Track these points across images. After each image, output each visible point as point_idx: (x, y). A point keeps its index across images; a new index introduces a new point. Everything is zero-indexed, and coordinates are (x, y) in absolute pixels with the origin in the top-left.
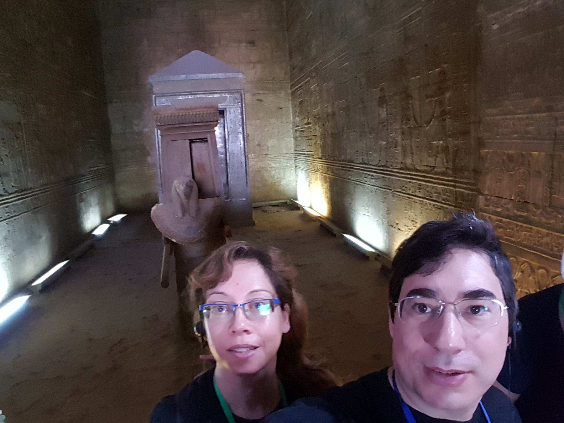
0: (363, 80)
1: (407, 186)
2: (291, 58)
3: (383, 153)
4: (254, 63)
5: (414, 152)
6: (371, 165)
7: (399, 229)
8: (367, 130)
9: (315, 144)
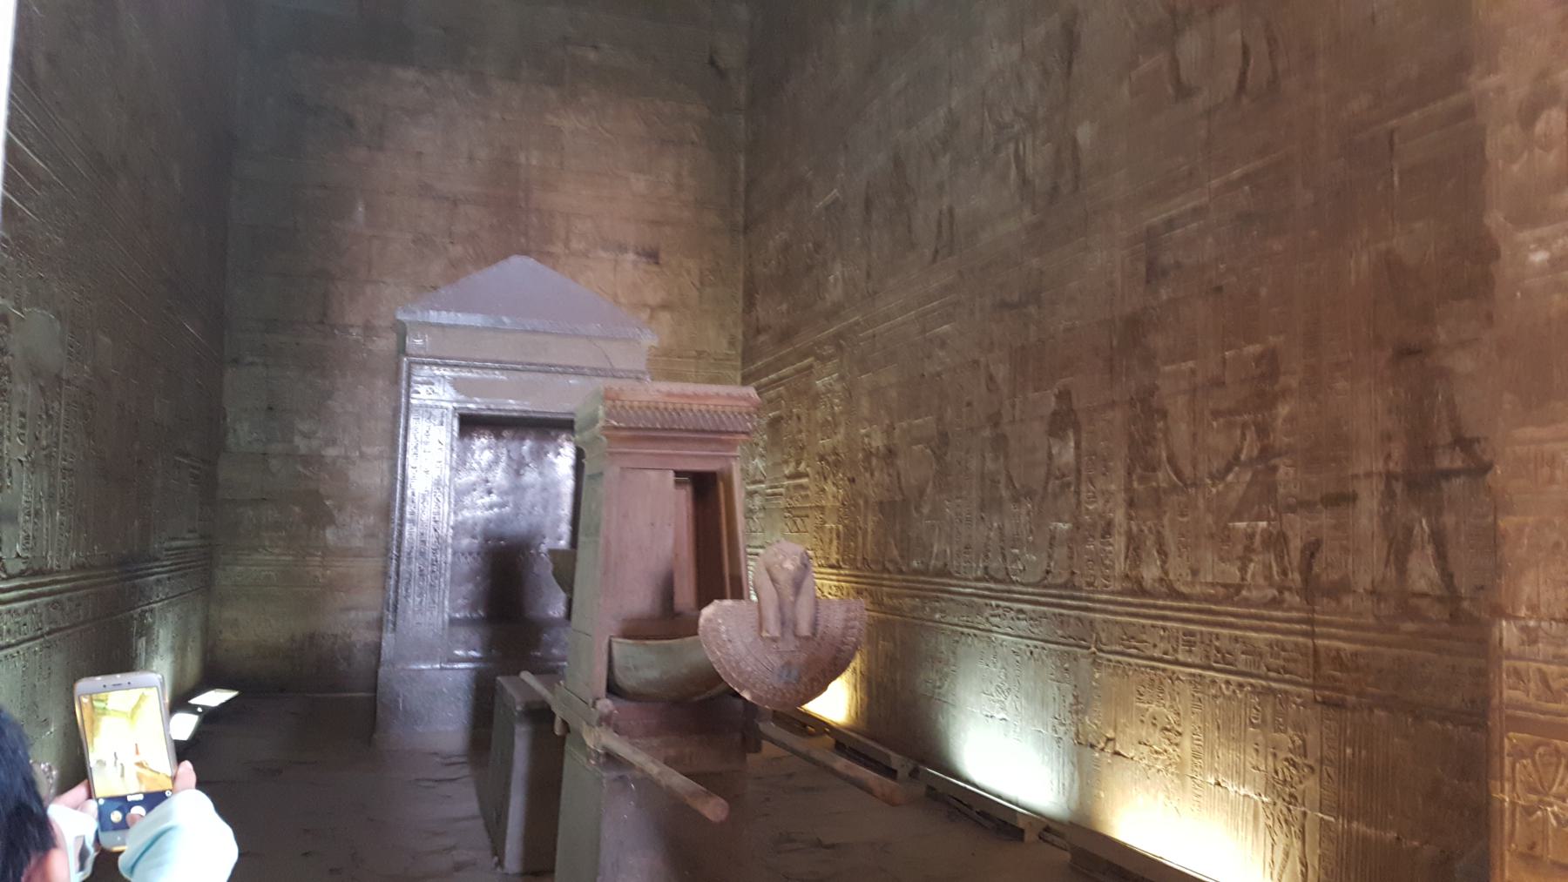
0: (1001, 372)
1: (1144, 637)
2: (750, 303)
3: (1061, 553)
4: (653, 309)
5: (1172, 548)
6: (1013, 582)
7: (1117, 753)
8: (1005, 493)
9: (820, 528)
